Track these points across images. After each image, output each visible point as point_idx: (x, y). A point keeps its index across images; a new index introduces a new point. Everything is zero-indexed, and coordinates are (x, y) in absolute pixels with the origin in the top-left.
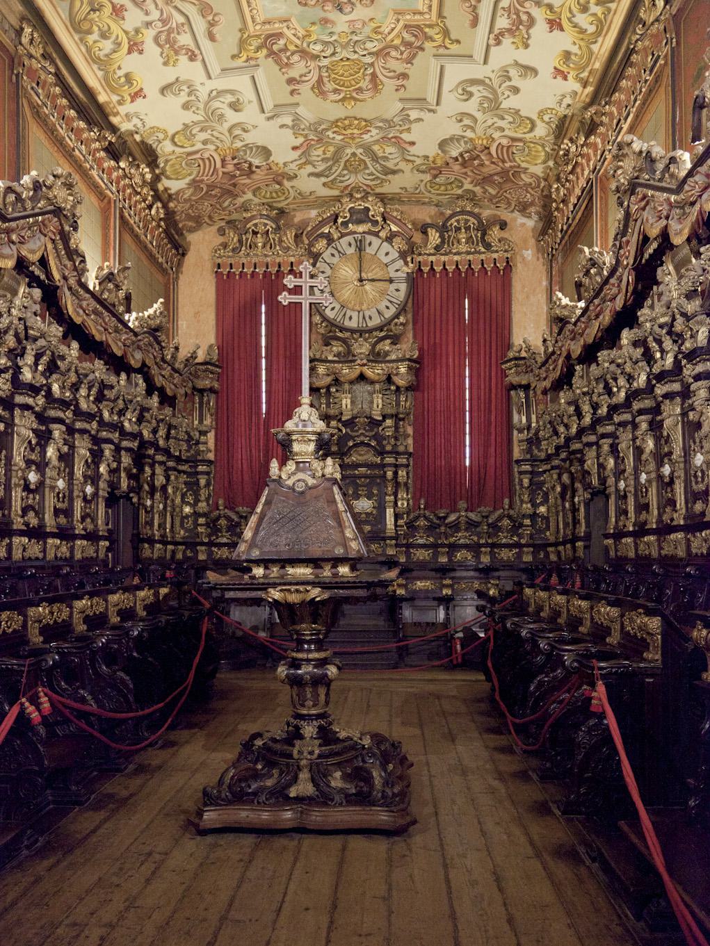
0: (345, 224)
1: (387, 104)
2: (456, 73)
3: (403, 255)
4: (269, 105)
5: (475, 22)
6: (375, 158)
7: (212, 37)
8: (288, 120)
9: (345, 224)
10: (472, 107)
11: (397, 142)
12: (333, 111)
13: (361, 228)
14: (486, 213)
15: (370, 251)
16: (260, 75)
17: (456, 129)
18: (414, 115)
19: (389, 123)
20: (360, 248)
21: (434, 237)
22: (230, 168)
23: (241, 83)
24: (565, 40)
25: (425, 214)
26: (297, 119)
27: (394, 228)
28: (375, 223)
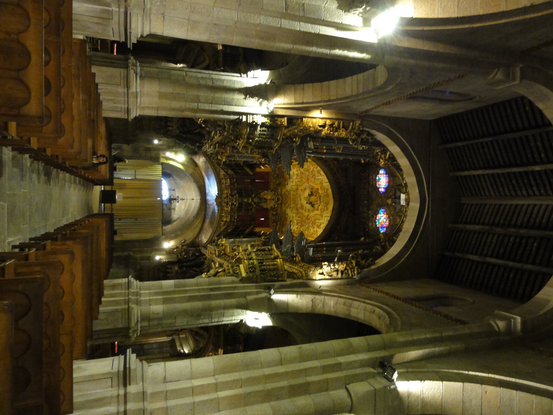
0: (277, 197)
1: (292, 206)
2: (294, 215)
3: (271, 207)
4: (293, 187)
5: (298, 217)
6: (287, 202)
7: (298, 181)
8: (291, 189)
9: (277, 197)
10: (291, 218)
11: (287, 207)
12: (292, 196)
13: (276, 200)
14: (279, 223)
15: (272, 201)
16: (295, 187)
17: (289, 216)
18: (291, 209)
19: (290, 205)
20: (273, 200)
21: (275, 213)
22: (286, 178)
23: (294, 184)
24: (296, 230)
25: (279, 211)
26: (291, 191)
27: (276, 206)
28: (277, 202)
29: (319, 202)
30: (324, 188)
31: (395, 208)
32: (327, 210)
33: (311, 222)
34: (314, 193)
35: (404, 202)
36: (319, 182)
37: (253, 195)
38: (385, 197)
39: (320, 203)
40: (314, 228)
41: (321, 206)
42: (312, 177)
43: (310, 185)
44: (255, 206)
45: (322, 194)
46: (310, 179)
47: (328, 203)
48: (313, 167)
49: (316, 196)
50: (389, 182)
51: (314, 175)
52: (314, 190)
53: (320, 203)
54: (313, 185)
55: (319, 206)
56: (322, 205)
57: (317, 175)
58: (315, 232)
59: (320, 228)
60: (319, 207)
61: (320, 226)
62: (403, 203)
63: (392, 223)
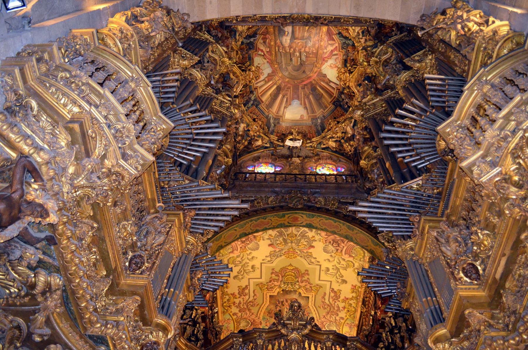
29: (295, 296)
30: (270, 282)
31: (306, 157)
32: (308, 274)
33: (329, 316)
34: (278, 309)
35: (298, 141)
36: (259, 293)
37: (283, 331)
38: (290, 167)
39: (295, 291)
40: (338, 307)
41: (300, 291)
42: (249, 310)
43: (264, 318)
44: (309, 327)
45: (280, 287)
46: (253, 317)
47: (296, 269)
48: (233, 307)
49: (282, 302)
50: (267, 163)
51: (247, 306)
52: (272, 307)
53: (295, 291)
54: (263, 311)
55: (300, 293)
56: (300, 287)
57: (247, 297)
58: (347, 306)
59: (340, 291)
60: (303, 295)
61: (335, 292)
62: (299, 143)
63: (329, 161)
